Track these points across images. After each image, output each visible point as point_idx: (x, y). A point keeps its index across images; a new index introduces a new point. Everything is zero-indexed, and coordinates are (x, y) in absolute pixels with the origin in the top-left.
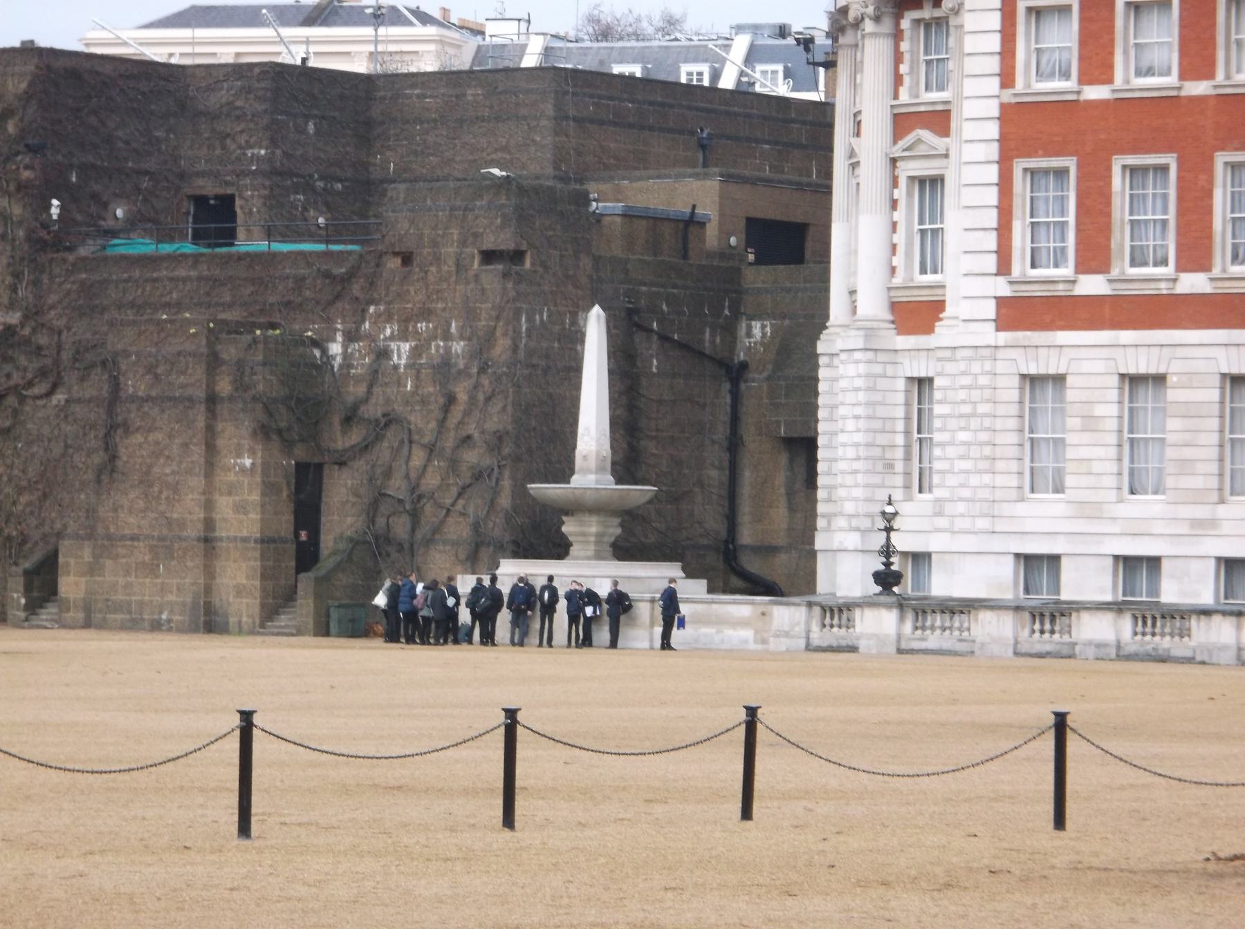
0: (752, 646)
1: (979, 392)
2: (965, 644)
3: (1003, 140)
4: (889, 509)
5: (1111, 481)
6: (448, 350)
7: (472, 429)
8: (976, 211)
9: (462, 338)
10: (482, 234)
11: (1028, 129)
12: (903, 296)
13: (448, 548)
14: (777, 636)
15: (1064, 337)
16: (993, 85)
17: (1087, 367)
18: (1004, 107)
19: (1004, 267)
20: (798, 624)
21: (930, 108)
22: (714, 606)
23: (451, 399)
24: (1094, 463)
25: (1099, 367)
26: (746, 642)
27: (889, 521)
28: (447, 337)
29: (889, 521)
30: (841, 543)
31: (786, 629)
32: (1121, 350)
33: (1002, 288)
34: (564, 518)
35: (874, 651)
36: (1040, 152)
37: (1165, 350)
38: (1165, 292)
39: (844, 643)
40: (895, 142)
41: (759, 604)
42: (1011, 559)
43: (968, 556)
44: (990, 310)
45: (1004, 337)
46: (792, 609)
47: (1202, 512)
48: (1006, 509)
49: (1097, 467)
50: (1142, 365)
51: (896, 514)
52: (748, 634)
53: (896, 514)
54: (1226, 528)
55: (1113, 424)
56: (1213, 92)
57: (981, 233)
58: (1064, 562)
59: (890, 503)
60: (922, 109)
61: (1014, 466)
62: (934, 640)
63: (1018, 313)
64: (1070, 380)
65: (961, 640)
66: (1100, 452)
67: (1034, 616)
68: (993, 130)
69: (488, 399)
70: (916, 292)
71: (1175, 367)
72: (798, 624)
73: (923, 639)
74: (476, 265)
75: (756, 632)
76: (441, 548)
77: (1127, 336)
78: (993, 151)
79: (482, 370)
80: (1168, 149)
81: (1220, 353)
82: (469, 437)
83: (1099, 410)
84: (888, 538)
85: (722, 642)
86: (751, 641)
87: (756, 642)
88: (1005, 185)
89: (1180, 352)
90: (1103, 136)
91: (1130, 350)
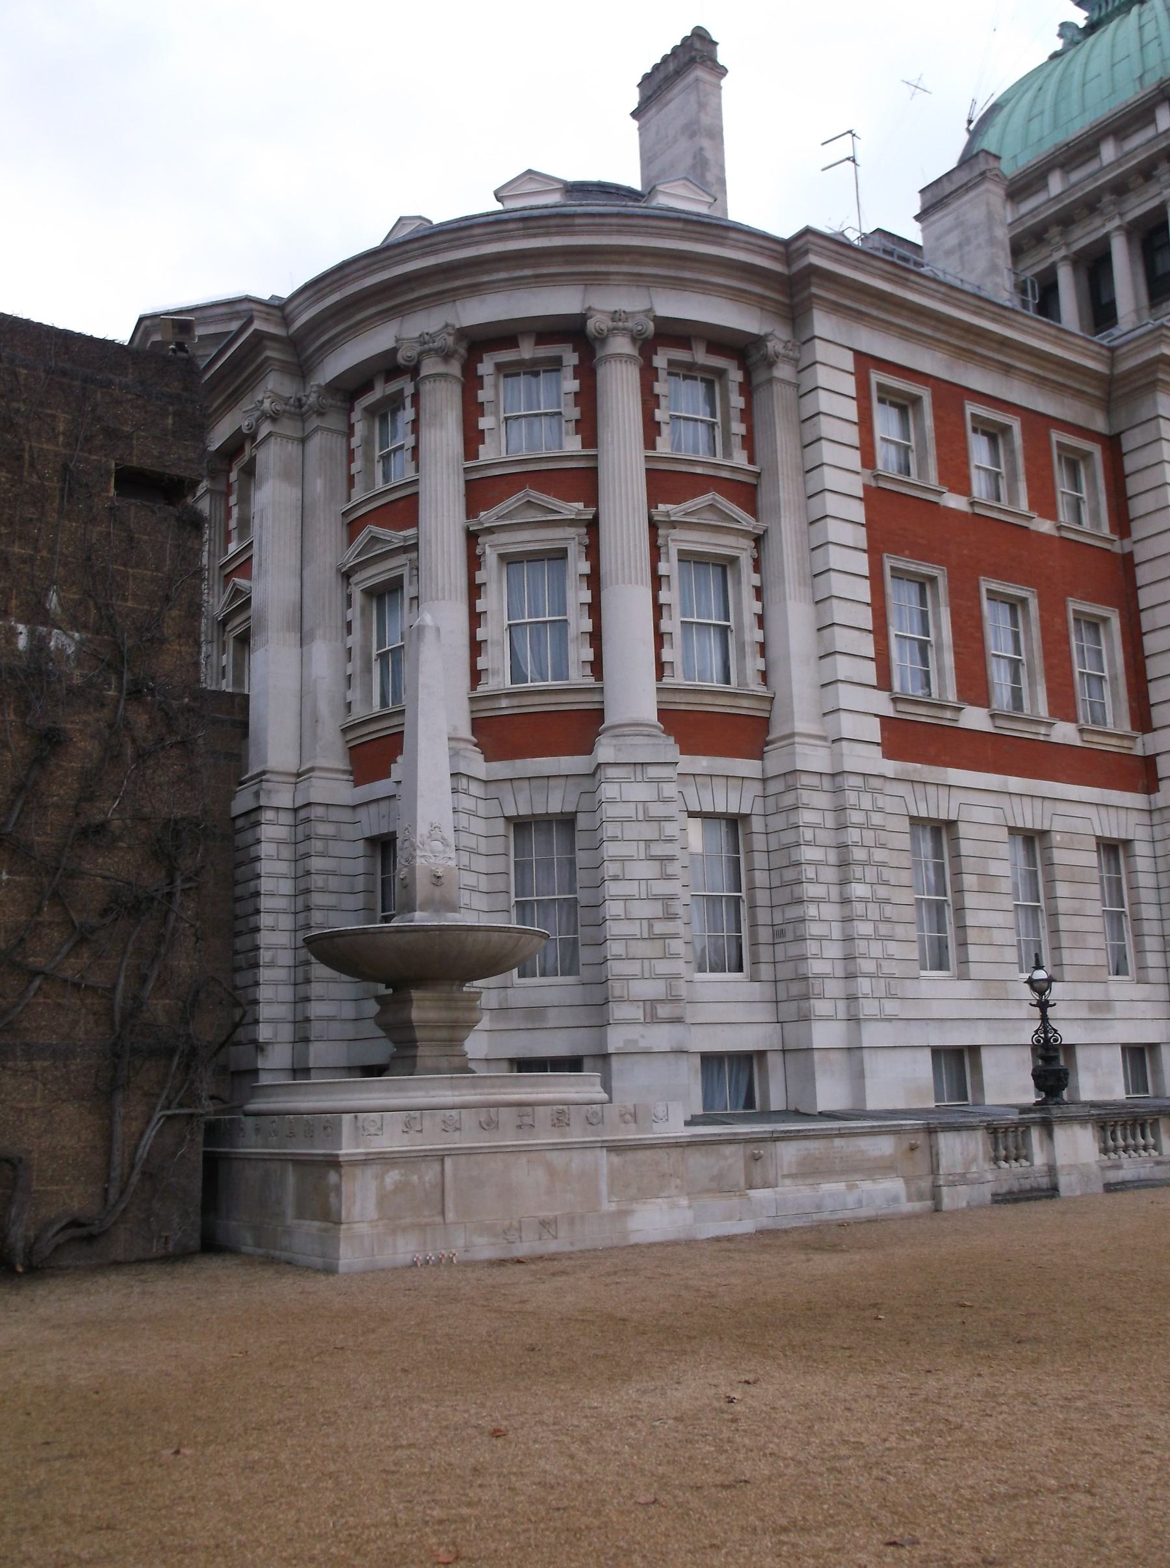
0: (907, 1207)
1: (871, 833)
2: (1163, 1167)
3: (869, 525)
4: (1040, 975)
5: (1011, 955)
6: (39, 644)
7: (108, 809)
8: (849, 604)
9: (75, 623)
10: (129, 437)
11: (895, 521)
12: (682, 703)
13: (38, 1064)
14: (952, 1184)
15: (956, 776)
16: (853, 459)
17: (979, 815)
18: (866, 488)
19: (884, 682)
20: (975, 1160)
21: (711, 472)
22: (838, 1142)
23: (51, 741)
24: (995, 932)
25: (988, 816)
26: (896, 1199)
27: (1041, 993)
28: (37, 615)
29: (1041, 993)
30: (627, 1042)
31: (959, 1170)
32: (1006, 798)
33: (882, 704)
34: (415, 994)
35: (1078, 1193)
36: (907, 552)
37: (1047, 803)
38: (1042, 738)
39: (1027, 1184)
40: (351, 539)
41: (907, 1132)
42: (927, 1056)
43: (879, 1052)
44: (873, 730)
45: (890, 767)
46: (964, 1134)
47: (1095, 992)
48: (910, 988)
49: (999, 937)
50: (1029, 817)
51: (1050, 980)
52: (894, 1185)
53: (1050, 980)
54: (1120, 1010)
55: (1006, 886)
56: (1055, 533)
57: (857, 633)
58: (986, 1057)
59: (1038, 966)
60: (699, 470)
61: (913, 933)
62: (1131, 1167)
63: (907, 738)
64: (963, 829)
65: (1158, 1163)
66: (997, 919)
67: (1103, 1128)
68: (858, 512)
69: (141, 756)
70: (708, 699)
71: (1057, 825)
72: (975, 1160)
73: (1118, 1167)
74: (112, 492)
75: (907, 1181)
76: (22, 1064)
77: (1015, 783)
78: (860, 537)
79: (136, 693)
80: (1027, 583)
81: (1091, 812)
82: (101, 828)
83: (995, 868)
84: (1044, 1019)
85: (860, 1203)
86: (903, 1199)
87: (910, 1199)
88: (876, 579)
89: (1062, 808)
90: (966, 552)
91: (1016, 800)
